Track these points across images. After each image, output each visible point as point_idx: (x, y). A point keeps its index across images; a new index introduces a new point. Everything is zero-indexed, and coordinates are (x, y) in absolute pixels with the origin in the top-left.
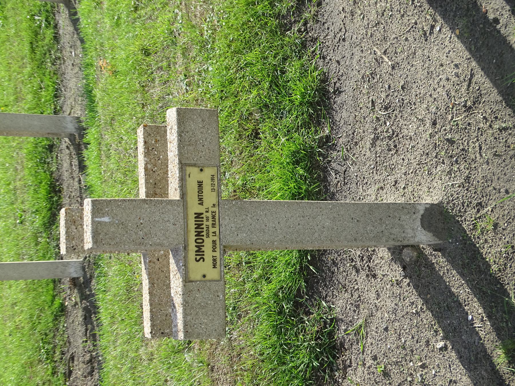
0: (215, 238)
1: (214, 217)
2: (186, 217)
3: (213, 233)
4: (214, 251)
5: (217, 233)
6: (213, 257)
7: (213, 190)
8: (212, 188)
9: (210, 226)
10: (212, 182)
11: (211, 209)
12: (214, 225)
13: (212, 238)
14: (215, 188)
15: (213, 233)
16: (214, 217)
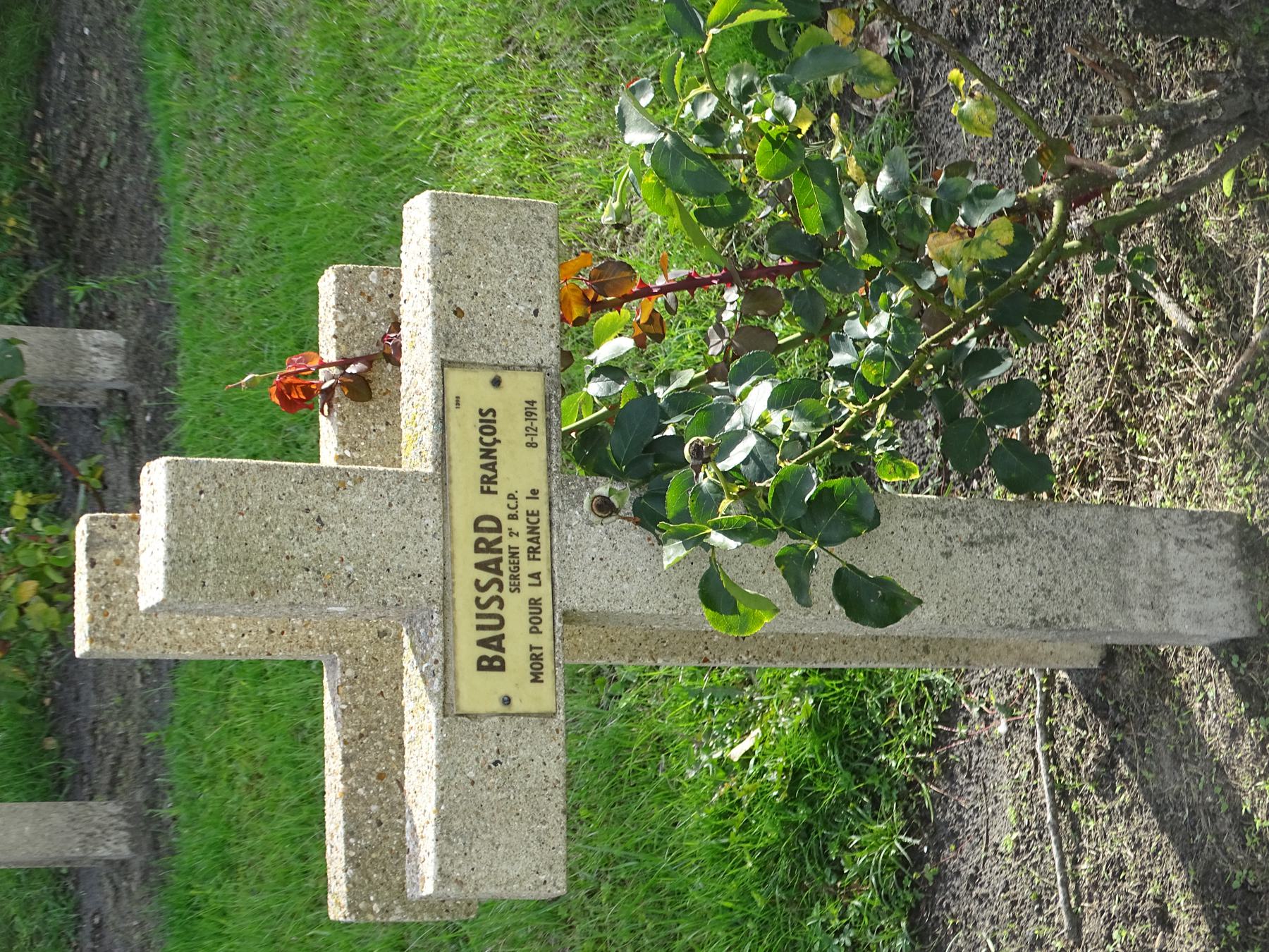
0: (535, 593)
1: (533, 529)
2: (446, 532)
3: (531, 576)
4: (535, 630)
5: (545, 577)
6: (531, 648)
7: (531, 445)
8: (528, 439)
9: (523, 555)
10: (528, 423)
11: (525, 505)
12: (533, 552)
13: (527, 592)
14: (536, 439)
15: (531, 576)
16: (533, 529)
